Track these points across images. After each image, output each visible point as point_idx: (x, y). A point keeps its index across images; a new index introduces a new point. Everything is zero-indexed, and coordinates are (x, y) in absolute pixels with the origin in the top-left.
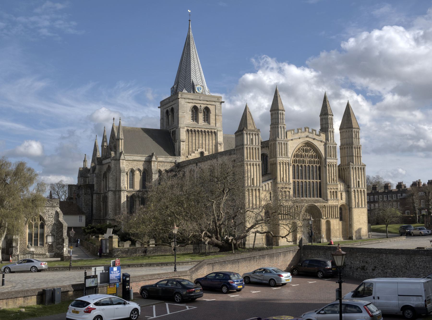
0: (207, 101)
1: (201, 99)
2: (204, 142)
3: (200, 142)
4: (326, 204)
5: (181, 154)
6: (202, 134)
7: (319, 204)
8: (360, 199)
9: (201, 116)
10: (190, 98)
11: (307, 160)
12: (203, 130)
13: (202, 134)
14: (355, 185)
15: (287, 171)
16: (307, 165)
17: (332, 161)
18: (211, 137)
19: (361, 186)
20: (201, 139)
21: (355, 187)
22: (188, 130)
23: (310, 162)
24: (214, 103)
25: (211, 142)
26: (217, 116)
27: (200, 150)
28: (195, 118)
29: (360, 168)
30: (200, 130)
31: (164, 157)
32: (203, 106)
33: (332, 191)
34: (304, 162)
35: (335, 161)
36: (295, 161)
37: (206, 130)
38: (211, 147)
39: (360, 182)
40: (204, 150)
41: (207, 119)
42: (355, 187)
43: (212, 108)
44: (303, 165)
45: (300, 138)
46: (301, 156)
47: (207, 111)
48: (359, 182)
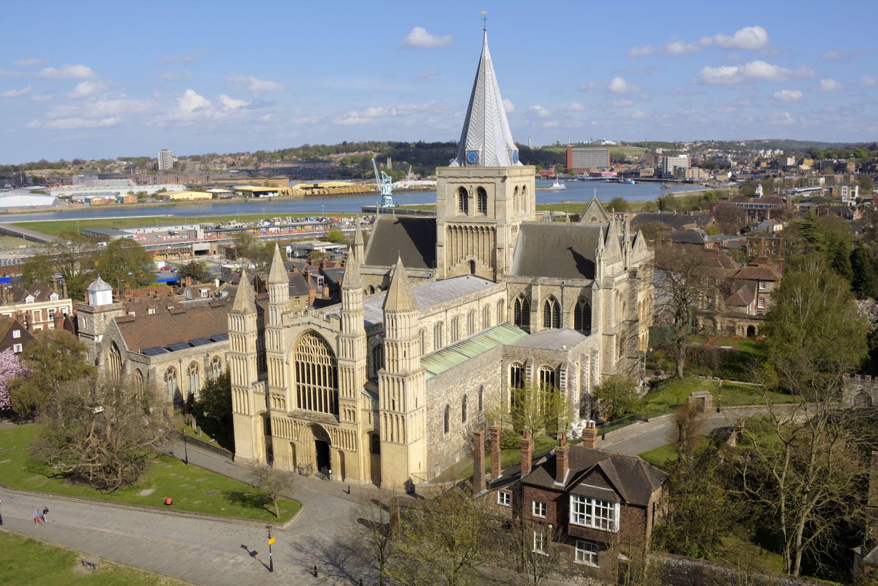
0: (480, 178)
1: (471, 175)
2: (475, 245)
3: (470, 245)
4: (336, 427)
5: (438, 265)
6: (472, 233)
7: (326, 425)
8: (395, 429)
9: (474, 203)
10: (453, 175)
11: (316, 355)
12: (473, 226)
13: (472, 233)
14: (387, 404)
15: (281, 374)
16: (316, 364)
17: (347, 363)
18: (486, 237)
19: (397, 409)
20: (471, 240)
21: (387, 408)
22: (450, 227)
23: (321, 359)
24: (491, 180)
25: (486, 245)
26: (497, 202)
27: (469, 258)
28: (464, 207)
29: (395, 379)
30: (468, 226)
31: (413, 269)
32: (475, 186)
33: (347, 408)
34: (311, 358)
35: (351, 363)
36: (299, 356)
37: (479, 226)
38: (486, 253)
39: (396, 403)
40: (477, 259)
41: (483, 208)
42: (387, 408)
43: (489, 189)
44: (310, 363)
45: (299, 325)
46: (308, 349)
47: (482, 192)
48: (393, 401)
